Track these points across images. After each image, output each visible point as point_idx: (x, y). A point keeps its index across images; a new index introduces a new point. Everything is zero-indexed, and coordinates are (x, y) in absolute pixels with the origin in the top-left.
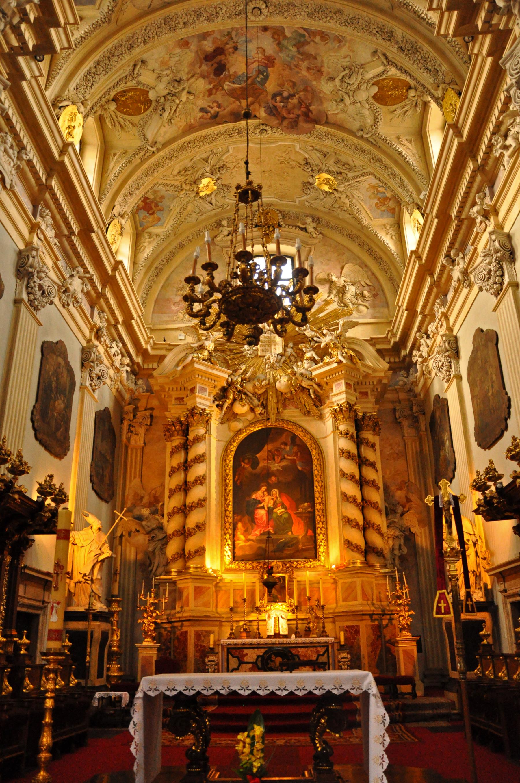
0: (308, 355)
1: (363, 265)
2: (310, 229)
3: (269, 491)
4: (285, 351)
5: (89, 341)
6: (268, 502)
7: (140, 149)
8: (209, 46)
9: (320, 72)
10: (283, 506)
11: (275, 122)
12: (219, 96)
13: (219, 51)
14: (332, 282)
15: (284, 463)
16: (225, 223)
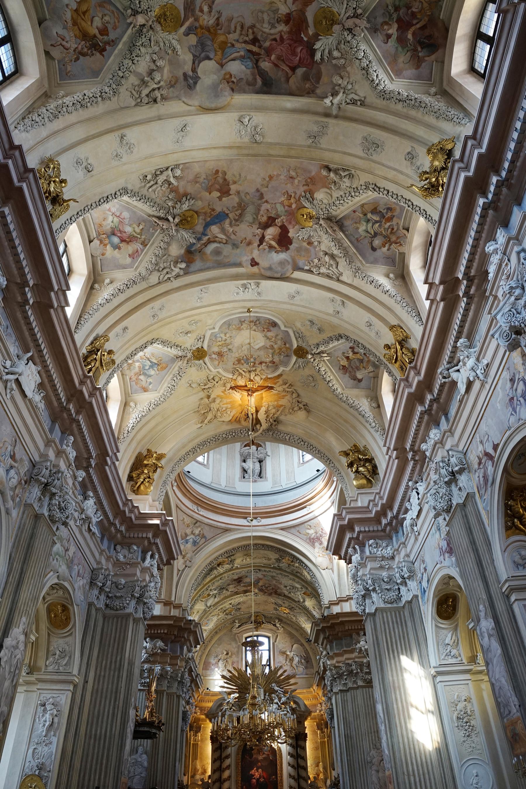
0: (276, 701)
1: (302, 645)
2: (278, 625)
3: (257, 770)
4: (265, 697)
5: (185, 708)
6: (257, 775)
7: (205, 610)
8: (236, 577)
9: (281, 583)
10: (264, 778)
11: (262, 593)
12: (238, 587)
13: (239, 578)
14: (287, 655)
15: (264, 756)
16: (237, 621)
